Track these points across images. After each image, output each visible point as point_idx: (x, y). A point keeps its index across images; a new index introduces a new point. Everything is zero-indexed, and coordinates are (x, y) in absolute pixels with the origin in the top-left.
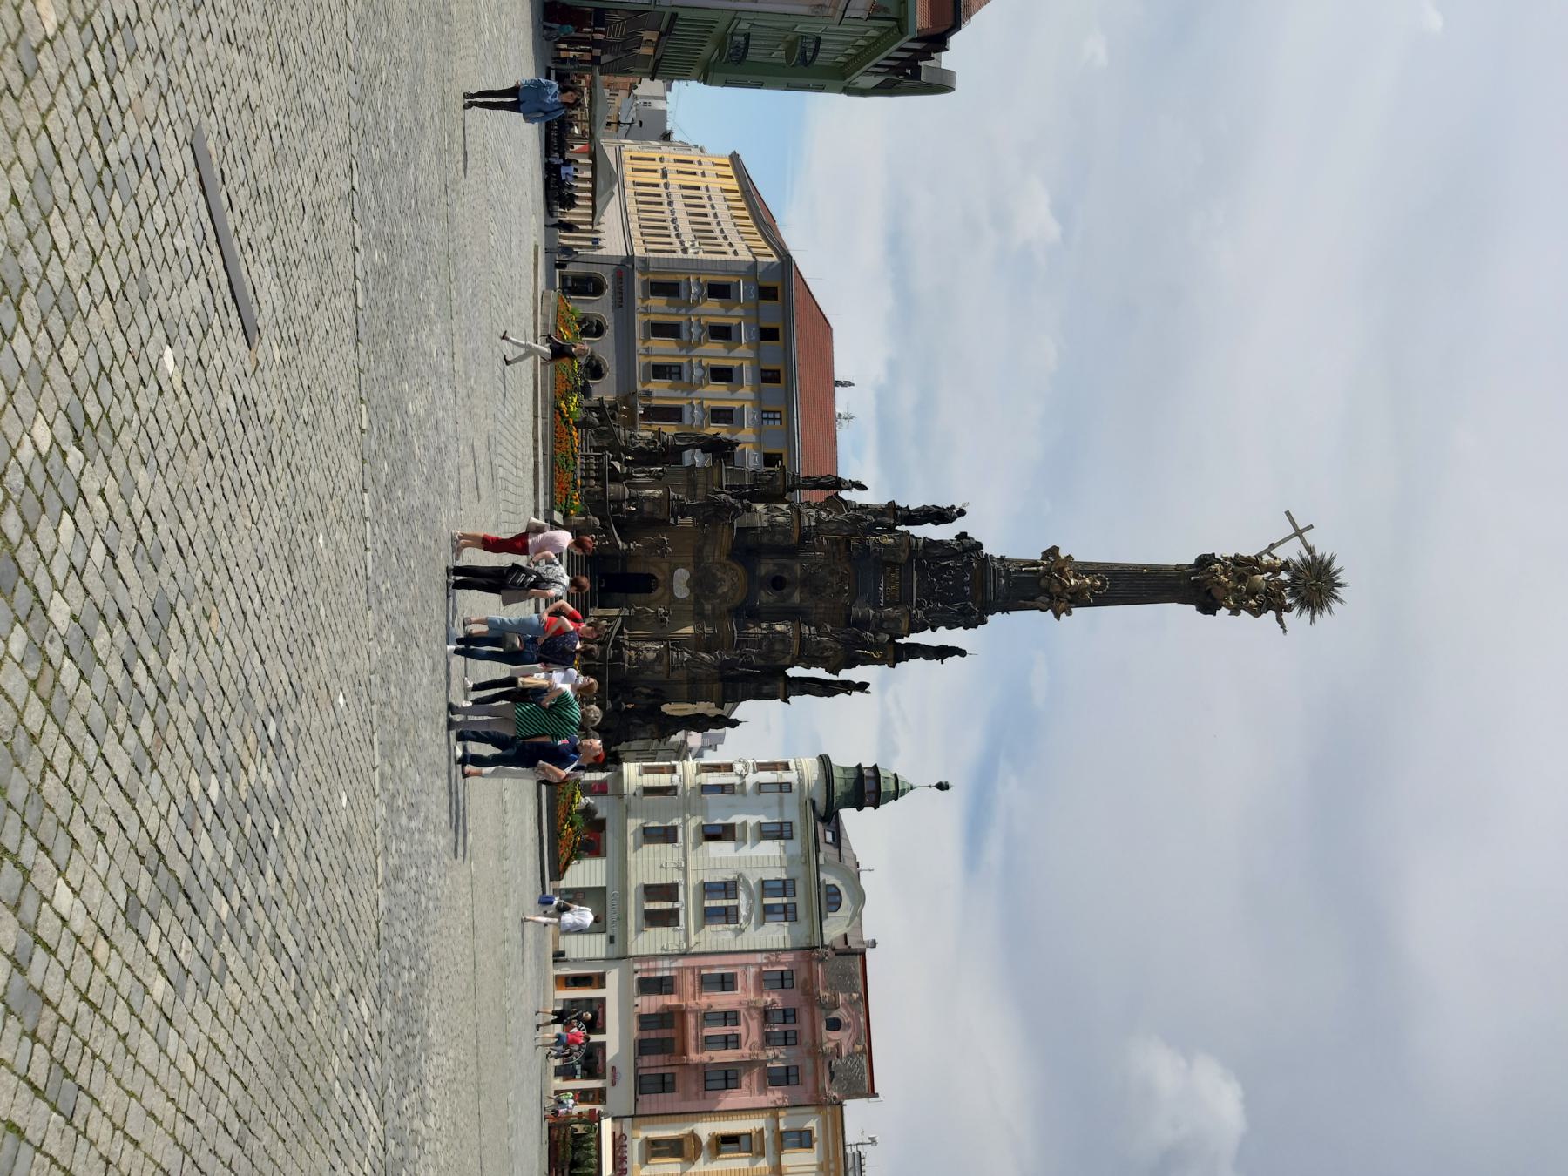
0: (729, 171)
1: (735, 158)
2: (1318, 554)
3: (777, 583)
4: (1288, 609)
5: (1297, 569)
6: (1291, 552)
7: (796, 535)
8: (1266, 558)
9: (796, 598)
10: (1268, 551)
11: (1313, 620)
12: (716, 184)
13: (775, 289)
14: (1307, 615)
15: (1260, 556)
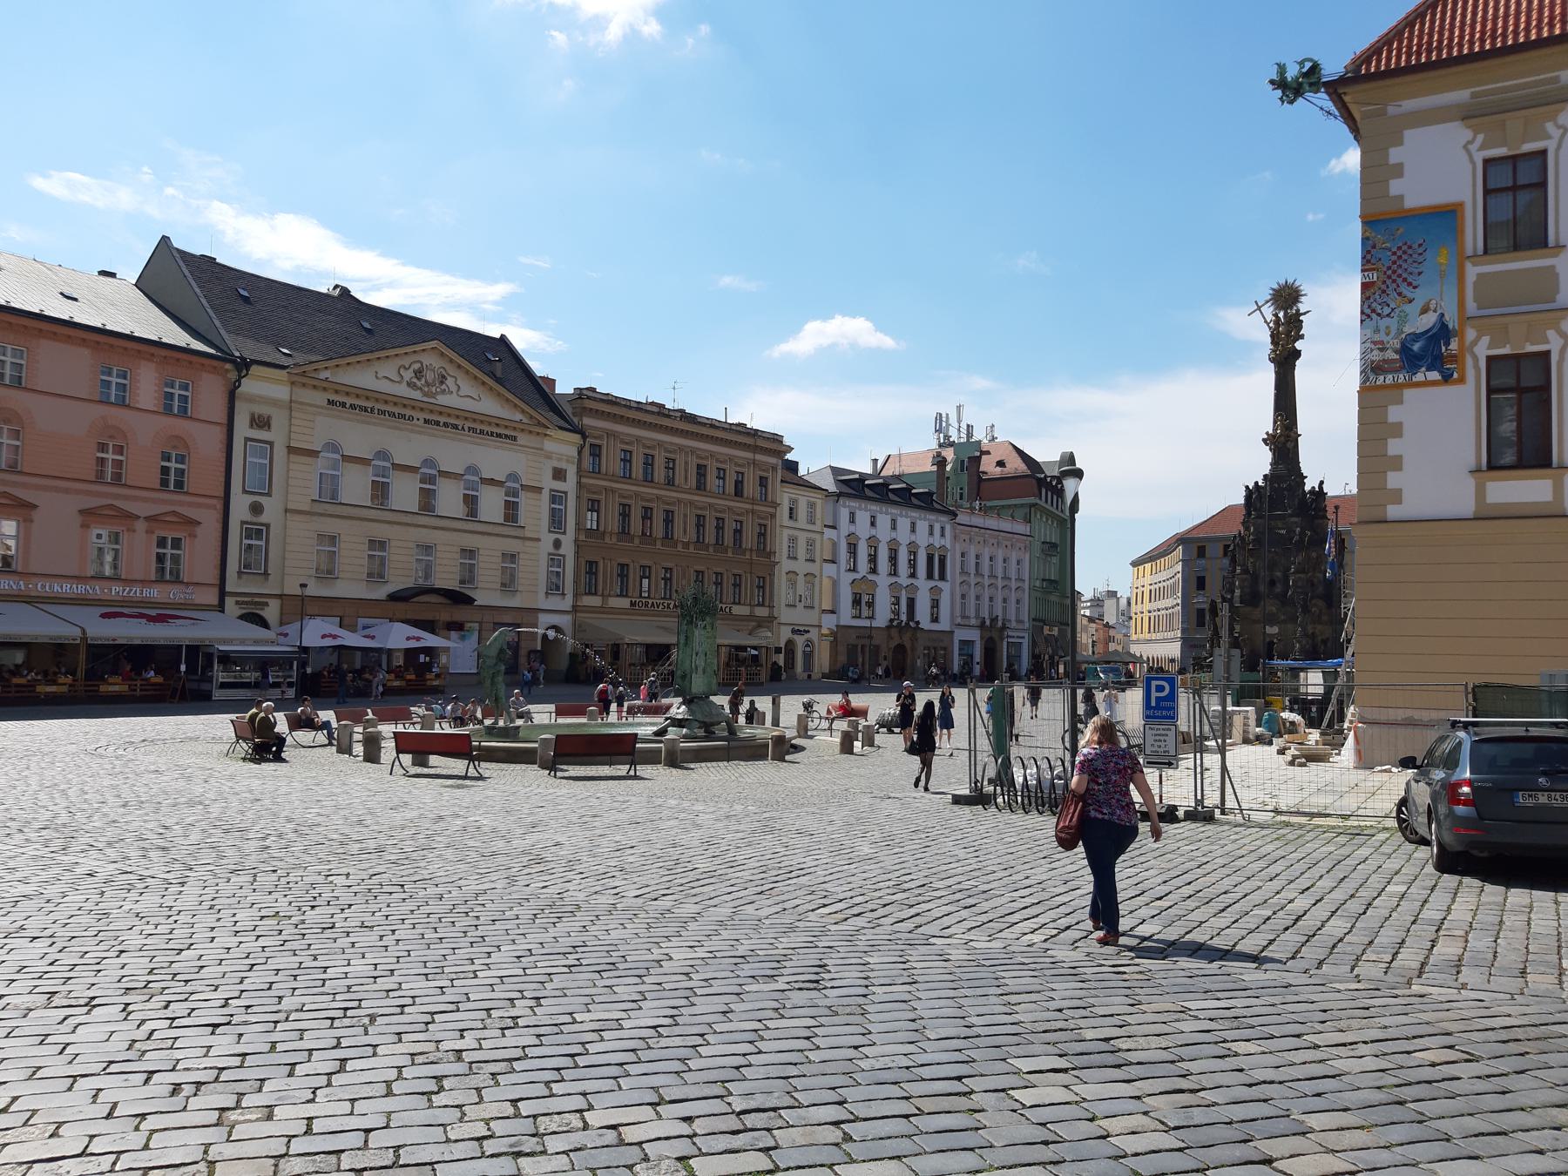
0: (1141, 568)
1: (1135, 564)
2: (1269, 297)
3: (1272, 583)
4: (1298, 310)
5: (1275, 309)
6: (1268, 311)
7: (1245, 576)
8: (1271, 325)
9: (1279, 574)
10: (1268, 324)
11: (1305, 295)
12: (1148, 579)
13: (1199, 547)
14: (1303, 299)
15: (1270, 328)
